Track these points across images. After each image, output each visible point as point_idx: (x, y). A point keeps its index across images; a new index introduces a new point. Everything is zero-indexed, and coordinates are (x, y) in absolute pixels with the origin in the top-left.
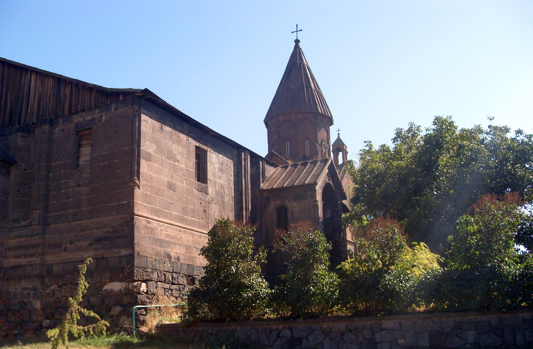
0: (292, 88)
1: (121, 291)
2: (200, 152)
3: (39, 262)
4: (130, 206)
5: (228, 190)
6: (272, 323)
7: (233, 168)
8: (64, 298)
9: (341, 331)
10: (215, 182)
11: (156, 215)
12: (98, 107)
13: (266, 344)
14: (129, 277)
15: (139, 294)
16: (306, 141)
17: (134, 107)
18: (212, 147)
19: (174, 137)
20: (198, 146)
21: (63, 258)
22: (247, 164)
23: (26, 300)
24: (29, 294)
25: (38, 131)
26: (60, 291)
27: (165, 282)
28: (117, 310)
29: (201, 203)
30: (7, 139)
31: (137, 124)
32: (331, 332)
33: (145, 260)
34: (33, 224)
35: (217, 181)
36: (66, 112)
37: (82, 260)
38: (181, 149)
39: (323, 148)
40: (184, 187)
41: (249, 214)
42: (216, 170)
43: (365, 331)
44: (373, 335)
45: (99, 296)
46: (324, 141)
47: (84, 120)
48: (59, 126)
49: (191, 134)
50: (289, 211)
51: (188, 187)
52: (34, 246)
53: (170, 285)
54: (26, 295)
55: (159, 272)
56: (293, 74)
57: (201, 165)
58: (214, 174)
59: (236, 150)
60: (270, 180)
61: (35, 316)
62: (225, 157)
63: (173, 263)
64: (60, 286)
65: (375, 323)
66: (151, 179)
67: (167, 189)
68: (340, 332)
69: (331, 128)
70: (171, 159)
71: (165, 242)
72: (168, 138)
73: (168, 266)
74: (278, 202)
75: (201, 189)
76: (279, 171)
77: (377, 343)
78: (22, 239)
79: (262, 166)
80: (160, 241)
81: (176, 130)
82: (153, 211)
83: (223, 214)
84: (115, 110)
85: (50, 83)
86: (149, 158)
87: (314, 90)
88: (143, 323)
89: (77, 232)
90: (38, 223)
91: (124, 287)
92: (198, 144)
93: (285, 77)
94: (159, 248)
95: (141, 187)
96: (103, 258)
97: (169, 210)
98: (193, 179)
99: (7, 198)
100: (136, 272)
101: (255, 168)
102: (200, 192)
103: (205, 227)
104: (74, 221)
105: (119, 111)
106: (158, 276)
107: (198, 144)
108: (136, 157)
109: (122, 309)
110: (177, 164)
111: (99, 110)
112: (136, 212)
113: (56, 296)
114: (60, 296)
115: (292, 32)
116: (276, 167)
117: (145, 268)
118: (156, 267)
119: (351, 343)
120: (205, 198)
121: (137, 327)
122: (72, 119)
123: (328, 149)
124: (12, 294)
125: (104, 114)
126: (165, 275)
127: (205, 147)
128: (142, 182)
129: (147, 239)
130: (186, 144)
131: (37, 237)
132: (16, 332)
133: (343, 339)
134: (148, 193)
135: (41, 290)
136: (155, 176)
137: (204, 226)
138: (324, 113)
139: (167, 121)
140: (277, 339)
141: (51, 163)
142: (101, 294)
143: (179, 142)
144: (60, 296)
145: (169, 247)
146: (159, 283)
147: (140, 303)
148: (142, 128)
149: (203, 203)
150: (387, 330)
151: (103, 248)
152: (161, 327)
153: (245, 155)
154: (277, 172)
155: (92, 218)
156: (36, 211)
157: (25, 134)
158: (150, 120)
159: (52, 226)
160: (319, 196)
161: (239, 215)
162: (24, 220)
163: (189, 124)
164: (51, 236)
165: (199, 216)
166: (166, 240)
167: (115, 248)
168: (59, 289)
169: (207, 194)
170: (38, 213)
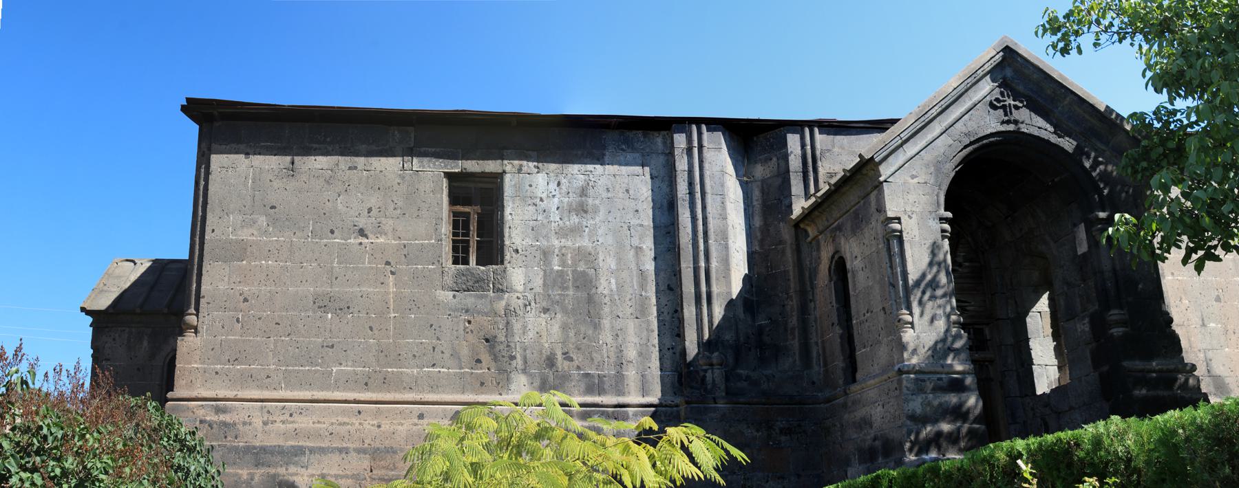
40: (387, 293)
70: (332, 232)
79: (803, 146)
83: (590, 332)
101: (775, 159)
102: (468, 290)
120: (492, 305)
137: (482, 384)
153: (690, 140)
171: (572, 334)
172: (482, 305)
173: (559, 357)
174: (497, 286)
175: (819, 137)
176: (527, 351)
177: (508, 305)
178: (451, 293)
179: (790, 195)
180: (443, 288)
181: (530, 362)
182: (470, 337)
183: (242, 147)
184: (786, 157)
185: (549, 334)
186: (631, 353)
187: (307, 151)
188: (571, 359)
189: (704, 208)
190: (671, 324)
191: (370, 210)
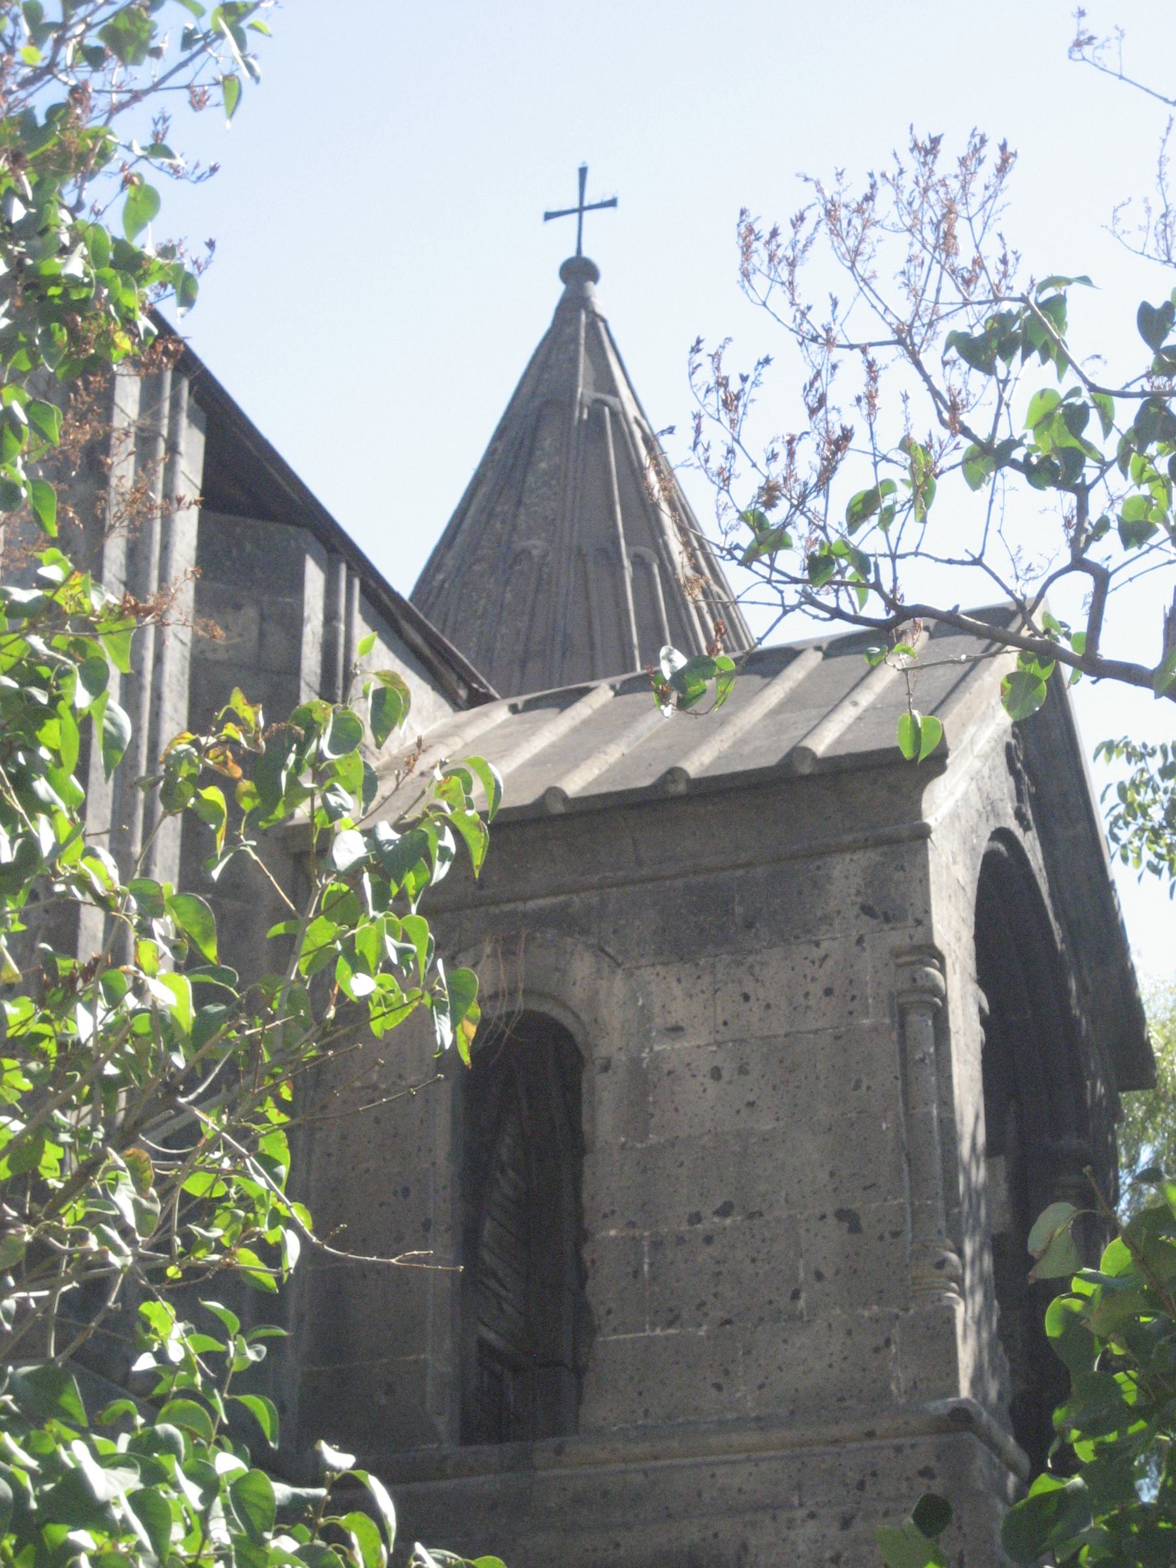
0: (535, 552)
50: (606, 1068)
56: (543, 465)
79: (330, 617)
93: (483, 490)
115: (549, 216)
184: (294, 623)
189: (159, 659)
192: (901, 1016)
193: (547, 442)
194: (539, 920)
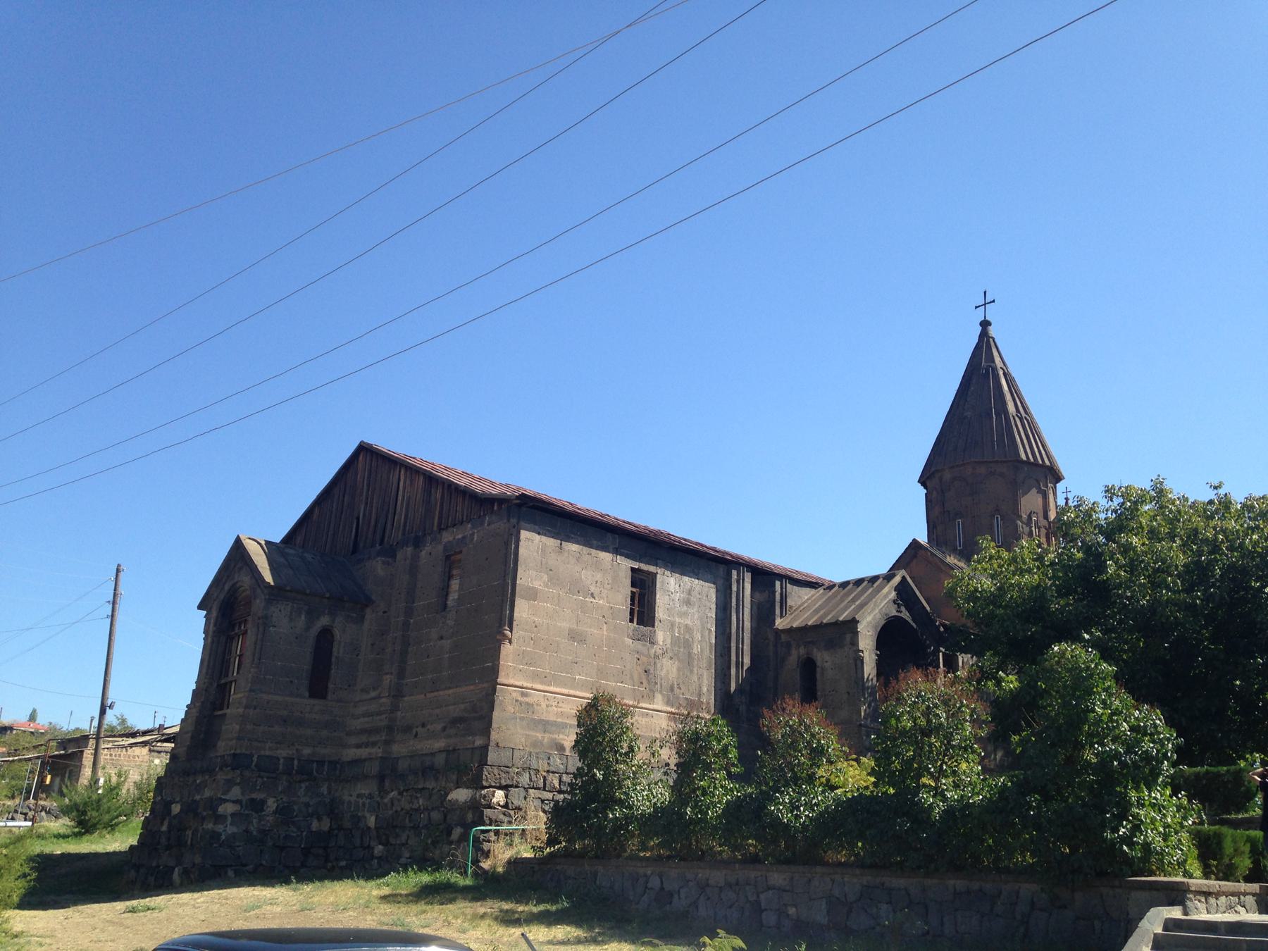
1: (466, 802)
2: (647, 577)
3: (380, 755)
4: (495, 671)
5: (702, 634)
6: (639, 864)
7: (714, 597)
8: (404, 811)
9: (719, 885)
10: (673, 625)
11: (542, 683)
12: (471, 519)
13: (631, 898)
14: (477, 783)
15: (490, 807)
16: (994, 516)
17: (511, 520)
18: (667, 566)
19: (586, 558)
20: (637, 567)
21: (411, 748)
22: (743, 588)
23: (359, 814)
24: (364, 804)
25: (399, 555)
26: (399, 800)
27: (544, 789)
28: (457, 832)
29: (638, 659)
30: (365, 566)
31: (513, 546)
32: (708, 885)
33: (509, 754)
34: (381, 695)
35: (677, 620)
36: (435, 528)
37: (431, 753)
38: (599, 576)
39: (1033, 529)
41: (742, 674)
42: (674, 604)
43: (747, 888)
44: (758, 896)
45: (443, 809)
46: (1035, 515)
47: (454, 539)
48: (426, 548)
49: (622, 550)
51: (612, 635)
52: (376, 731)
53: (554, 795)
54: (361, 805)
55: (532, 773)
57: (646, 597)
58: (669, 610)
59: (723, 566)
60: (796, 612)
61: (368, 839)
62: (697, 580)
63: (567, 759)
64: (401, 793)
65: (761, 876)
66: (536, 627)
67: (566, 641)
68: (717, 887)
69: (1060, 487)
71: (554, 724)
72: (573, 561)
73: (557, 762)
74: (802, 651)
75: (640, 636)
76: (818, 594)
77: (763, 911)
78: (366, 719)
79: (782, 588)
80: (544, 723)
81: (591, 547)
82: (535, 676)
83: (688, 674)
84: (489, 525)
85: (420, 481)
86: (533, 595)
87: (1013, 416)
88: (487, 854)
89: (432, 709)
90: (387, 695)
91: (470, 796)
92: (636, 565)
94: (539, 735)
95: (514, 640)
96: (454, 750)
97: (569, 673)
98: (624, 621)
99: (357, 656)
100: (485, 773)
102: (639, 640)
103: (645, 697)
104: (432, 692)
105: (493, 526)
106: (531, 780)
107: (636, 565)
108: (509, 596)
109: (462, 830)
110: (589, 599)
111: (471, 524)
112: (499, 680)
113: (394, 809)
114: (399, 809)
116: (816, 588)
117: (508, 767)
118: (530, 764)
119: (730, 907)
121: (476, 862)
122: (441, 536)
123: (1046, 529)
124: (346, 804)
125: (476, 531)
126: (544, 778)
127: (652, 569)
128: (517, 633)
129: (518, 720)
130: (610, 567)
131: (384, 716)
132: (343, 863)
133: (721, 899)
134: (528, 649)
135: (378, 799)
136: (543, 622)
138: (1032, 460)
139: (573, 536)
140: (645, 892)
141: (413, 602)
142: (444, 807)
143: (597, 566)
144: (399, 809)
145: (563, 733)
146: (531, 791)
147: (488, 822)
148: (522, 550)
149: (643, 659)
150: (774, 889)
151: (456, 734)
152: (514, 863)
153: (738, 575)
154: (814, 598)
155: (450, 688)
156: (388, 676)
157: (387, 559)
158: (537, 537)
159: (406, 699)
160: (867, 642)
161: (725, 675)
162: (374, 689)
163: (618, 534)
164: (403, 714)
165: (633, 681)
166: (555, 721)
167: (469, 736)
168: (399, 797)
169: (652, 643)
170: (389, 680)
171: (681, 673)
172: (644, 650)
173: (676, 686)
174: (652, 640)
175: (788, 585)
176: (663, 681)
177: (655, 652)
178: (632, 640)
179: (775, 615)
180: (628, 637)
181: (663, 688)
182: (639, 668)
183: (537, 527)
184: (774, 592)
185: (672, 672)
186: (705, 689)
187: (568, 539)
188: (680, 689)
189: (743, 614)
190: (722, 675)
191: (597, 582)
192: (855, 660)
193: (974, 381)
194: (809, 642)
